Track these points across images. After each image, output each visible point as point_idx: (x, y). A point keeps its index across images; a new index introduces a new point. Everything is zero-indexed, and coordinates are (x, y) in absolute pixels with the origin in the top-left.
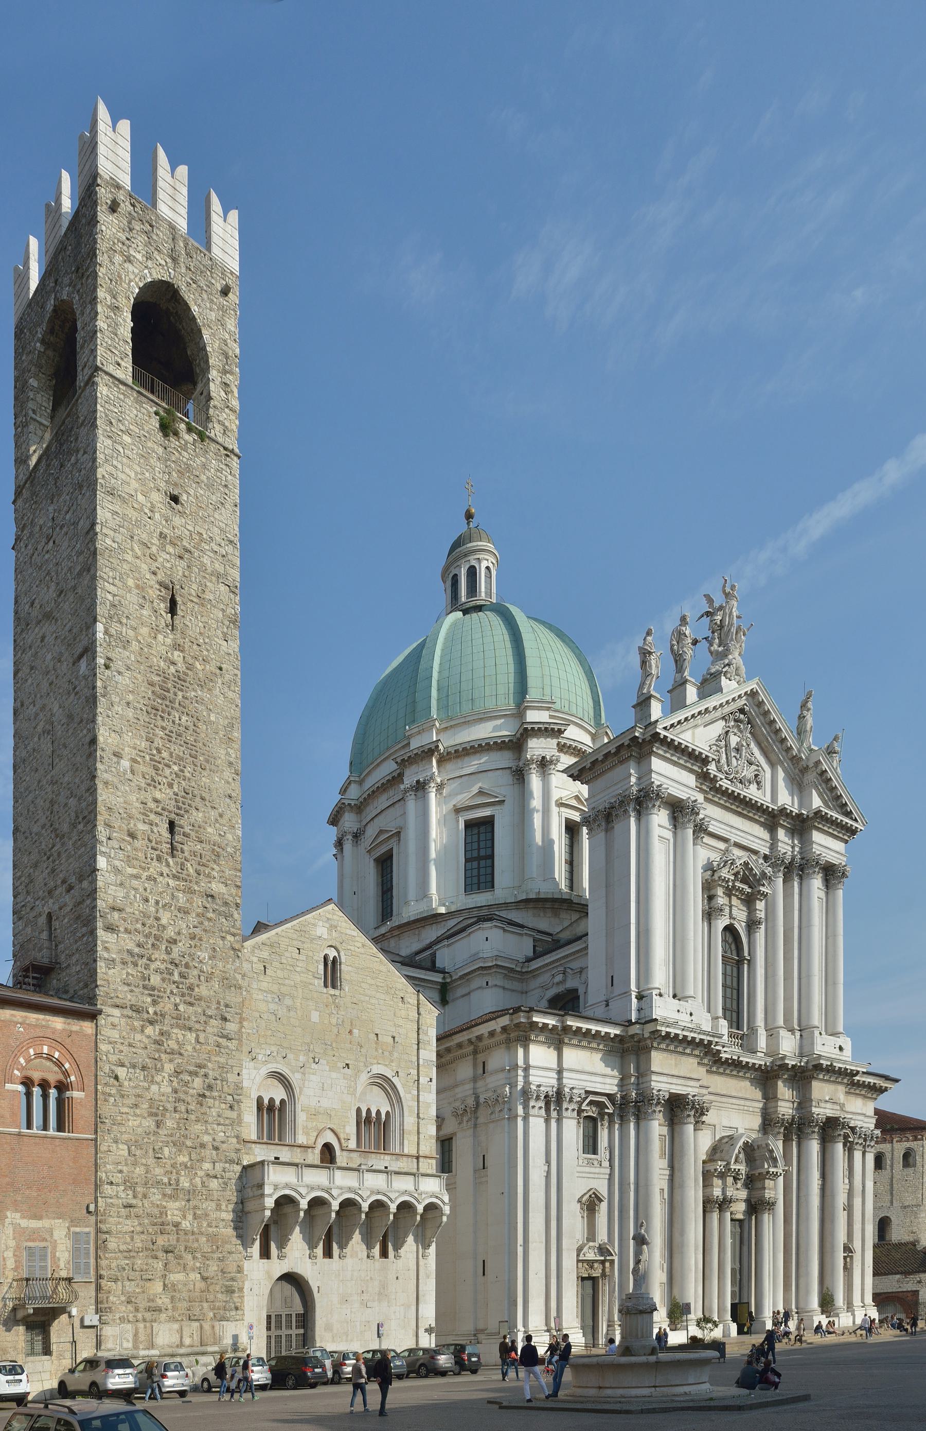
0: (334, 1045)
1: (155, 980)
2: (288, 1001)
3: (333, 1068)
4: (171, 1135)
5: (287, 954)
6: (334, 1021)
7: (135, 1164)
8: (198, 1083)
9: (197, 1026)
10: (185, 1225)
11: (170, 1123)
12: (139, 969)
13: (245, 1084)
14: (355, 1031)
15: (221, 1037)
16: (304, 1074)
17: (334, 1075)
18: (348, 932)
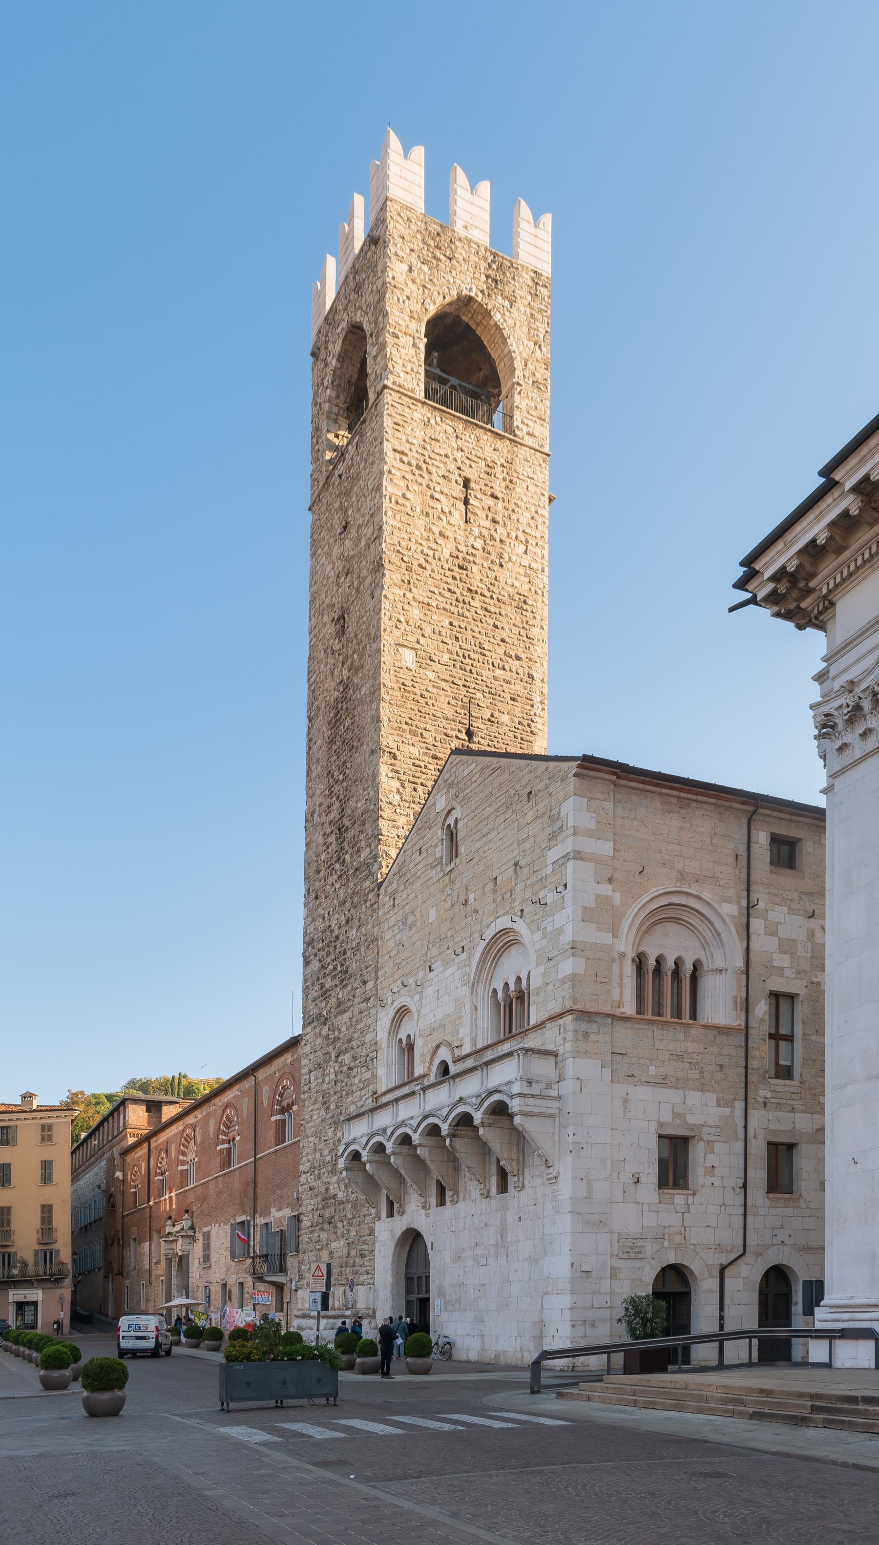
0: (449, 934)
1: (328, 983)
2: (410, 920)
3: (446, 964)
4: (333, 1117)
5: (412, 865)
6: (449, 904)
7: (315, 1151)
8: (346, 1058)
9: (349, 1004)
10: (340, 1195)
11: (331, 1107)
12: (321, 981)
13: (379, 1037)
14: (471, 897)
15: (363, 1002)
16: (422, 992)
17: (449, 972)
18: (466, 772)
